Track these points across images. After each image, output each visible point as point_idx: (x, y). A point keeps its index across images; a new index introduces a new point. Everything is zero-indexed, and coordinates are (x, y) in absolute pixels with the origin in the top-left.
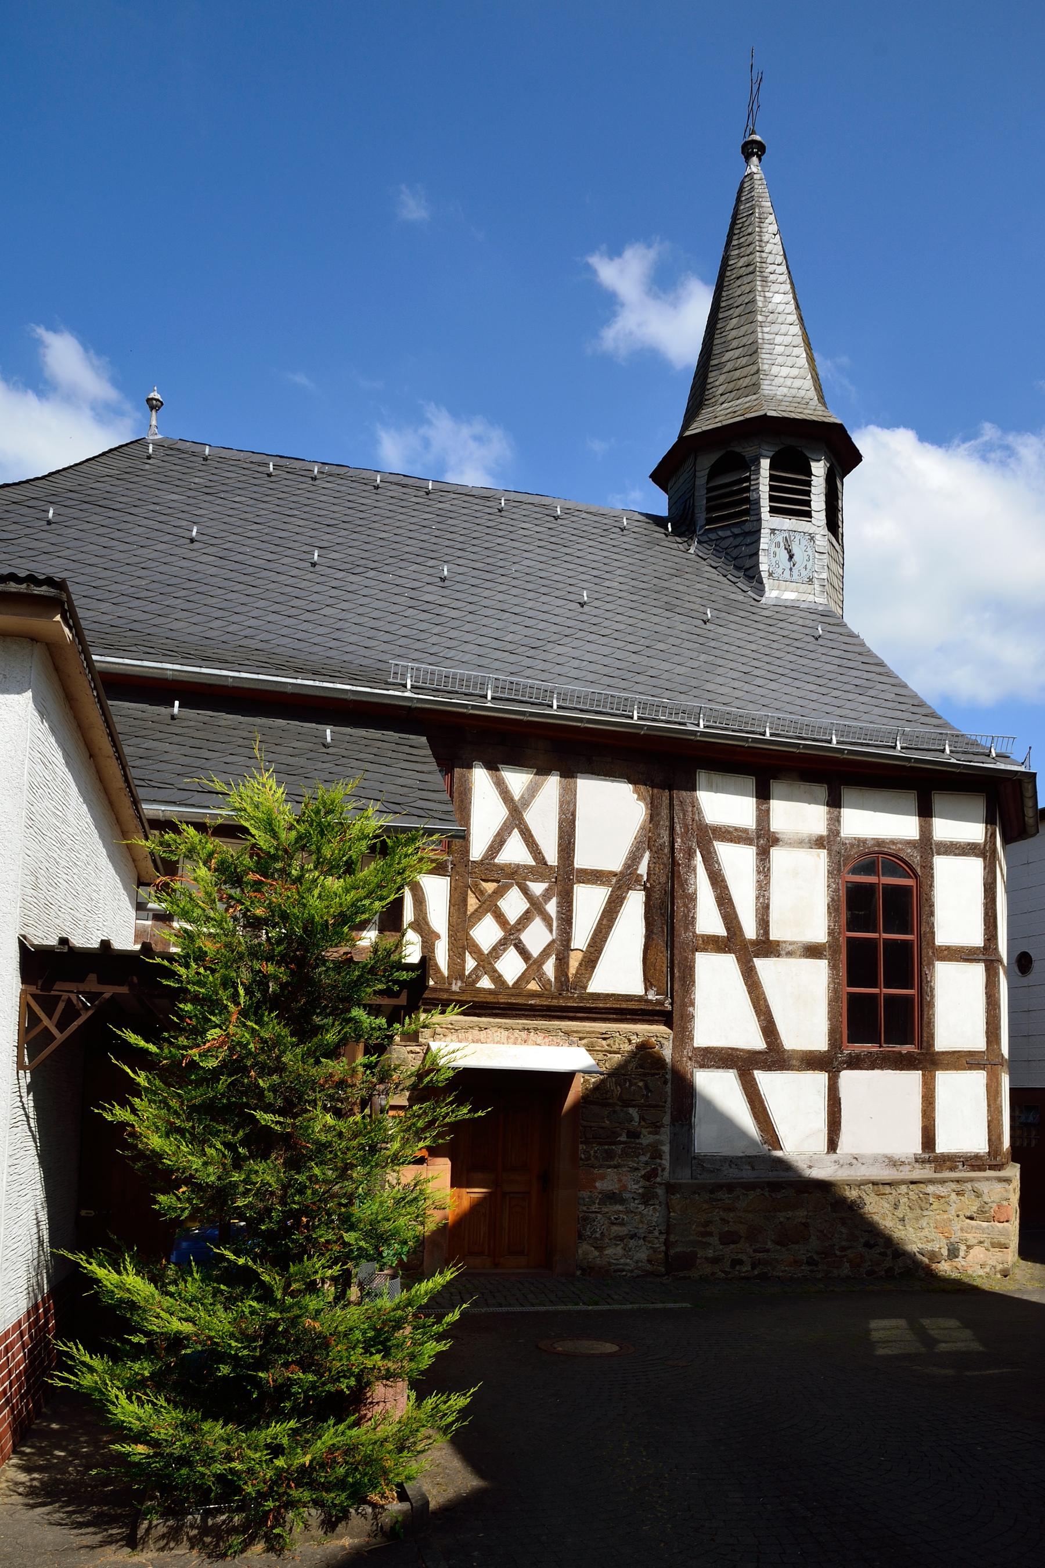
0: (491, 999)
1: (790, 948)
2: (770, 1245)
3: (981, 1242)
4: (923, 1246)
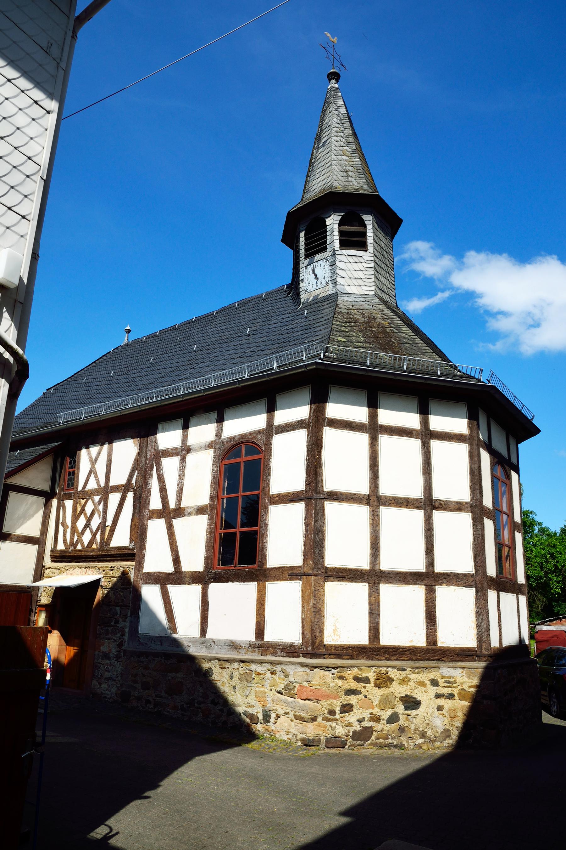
0: (80, 554)
1: (190, 510)
2: (163, 693)
3: (287, 713)
4: (247, 709)
